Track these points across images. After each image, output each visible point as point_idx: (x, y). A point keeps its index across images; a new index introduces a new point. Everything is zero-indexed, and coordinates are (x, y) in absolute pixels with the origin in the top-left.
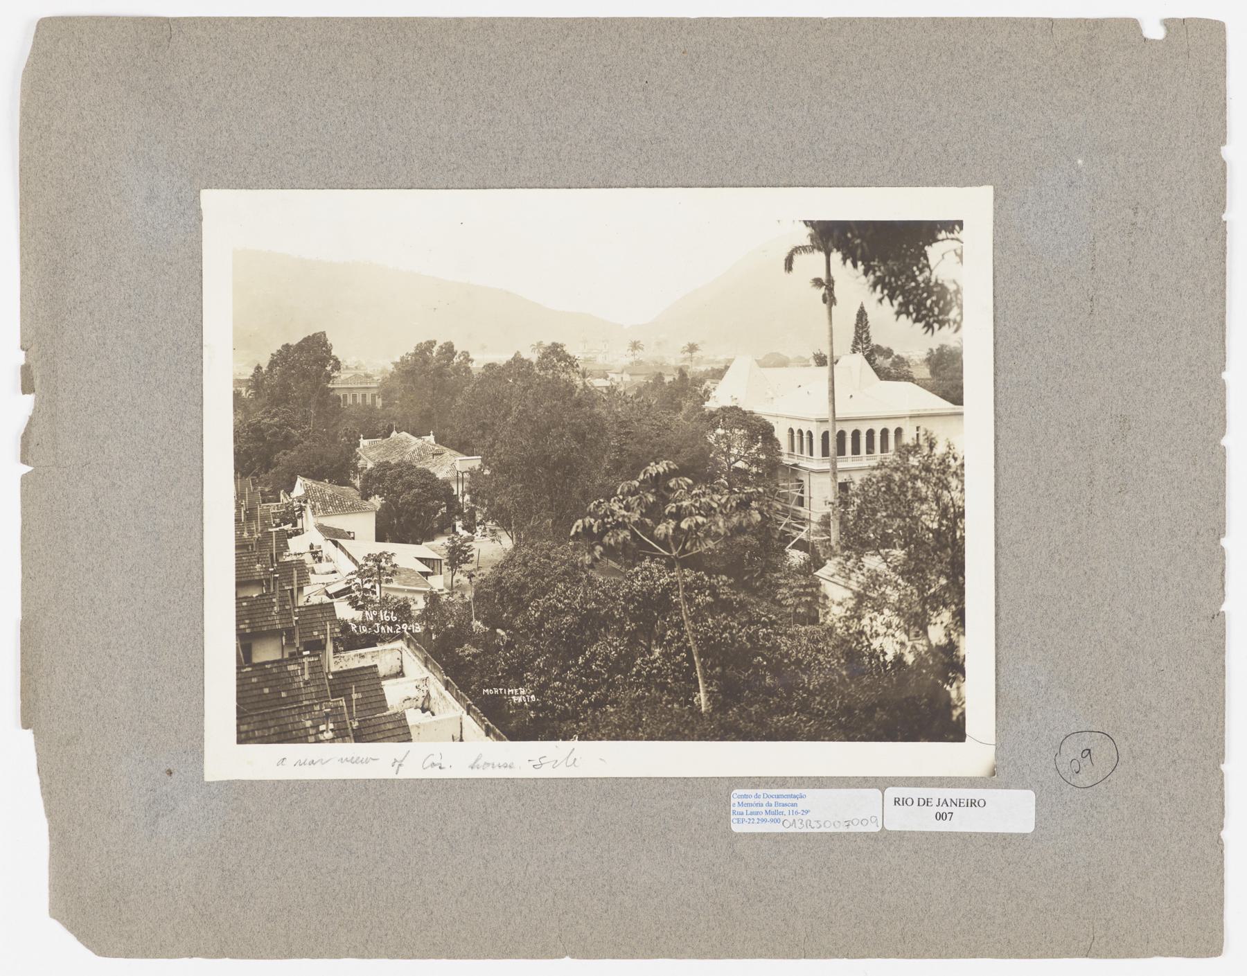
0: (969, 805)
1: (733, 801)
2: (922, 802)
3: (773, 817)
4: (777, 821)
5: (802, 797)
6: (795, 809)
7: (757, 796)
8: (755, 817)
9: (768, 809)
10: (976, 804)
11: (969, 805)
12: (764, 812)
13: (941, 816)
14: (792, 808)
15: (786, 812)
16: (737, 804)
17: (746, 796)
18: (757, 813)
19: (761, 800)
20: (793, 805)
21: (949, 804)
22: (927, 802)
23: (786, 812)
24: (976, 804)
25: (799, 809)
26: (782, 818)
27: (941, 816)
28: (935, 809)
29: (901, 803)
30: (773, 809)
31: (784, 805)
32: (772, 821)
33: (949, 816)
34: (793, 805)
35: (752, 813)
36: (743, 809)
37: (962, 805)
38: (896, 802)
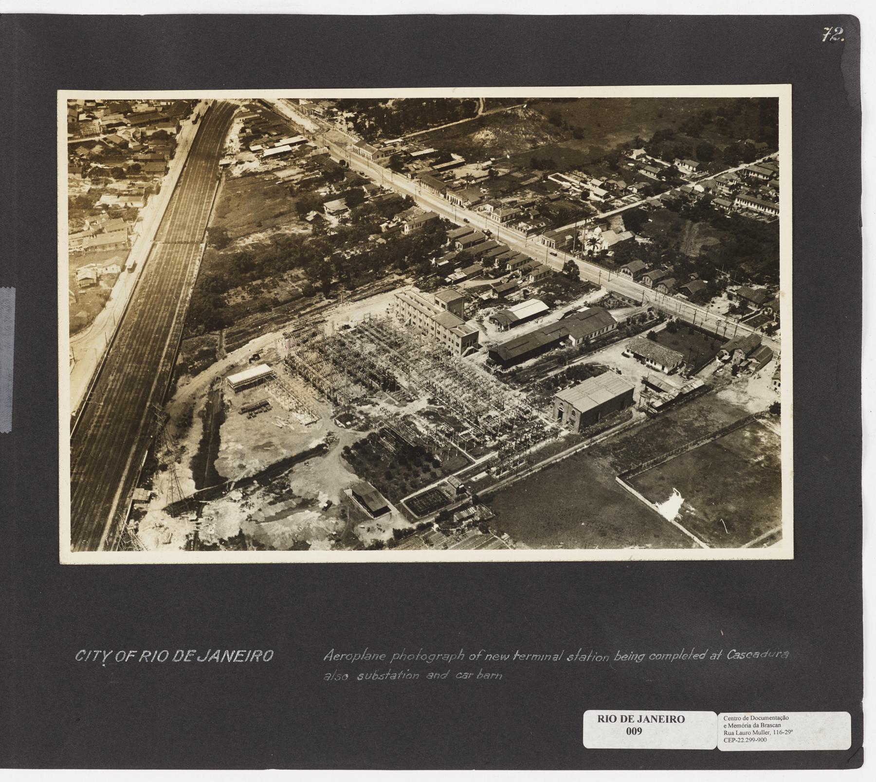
5: (785, 718)
6: (779, 729)
7: (747, 719)
8: (745, 737)
9: (755, 729)
12: (752, 732)
14: (776, 729)
15: (772, 732)
16: (728, 725)
17: (735, 719)
20: (779, 726)
23: (772, 732)
30: (760, 729)
31: (768, 726)
34: (779, 726)
35: (741, 734)
36: (733, 730)
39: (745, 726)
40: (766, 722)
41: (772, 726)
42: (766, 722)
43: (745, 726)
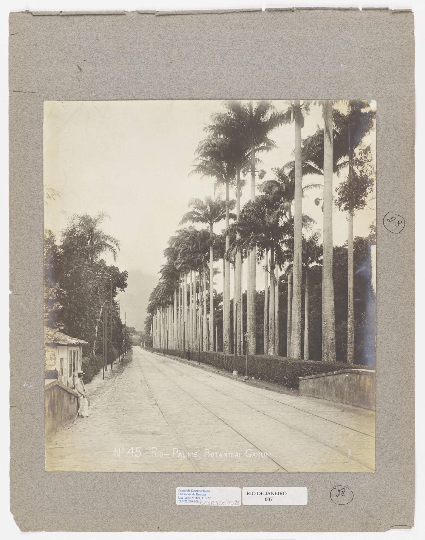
0: (279, 494)
1: (177, 493)
2: (259, 493)
3: (196, 500)
4: (197, 502)
5: (208, 491)
6: (205, 496)
8: (188, 500)
9: (193, 496)
10: (282, 494)
11: (279, 494)
13: (267, 499)
15: (201, 498)
17: (184, 491)
18: (188, 498)
19: (190, 493)
20: (205, 495)
21: (271, 494)
22: (261, 494)
23: (201, 498)
24: (282, 494)
25: (207, 496)
26: (199, 500)
27: (267, 499)
28: (264, 497)
29: (250, 494)
30: (195, 496)
32: (195, 501)
33: (271, 499)
35: (186, 498)
36: (183, 496)
37: (276, 494)
38: (248, 493)
39: (188, 494)
40: (199, 493)
41: (201, 495)
42: (199, 493)
43: (188, 494)
